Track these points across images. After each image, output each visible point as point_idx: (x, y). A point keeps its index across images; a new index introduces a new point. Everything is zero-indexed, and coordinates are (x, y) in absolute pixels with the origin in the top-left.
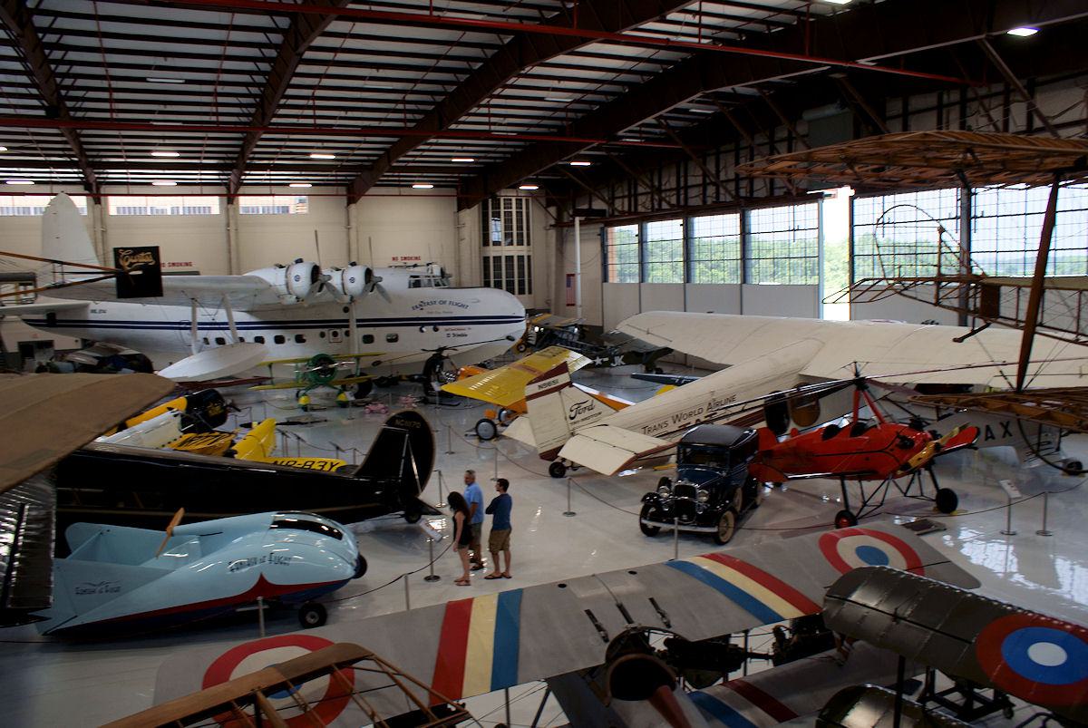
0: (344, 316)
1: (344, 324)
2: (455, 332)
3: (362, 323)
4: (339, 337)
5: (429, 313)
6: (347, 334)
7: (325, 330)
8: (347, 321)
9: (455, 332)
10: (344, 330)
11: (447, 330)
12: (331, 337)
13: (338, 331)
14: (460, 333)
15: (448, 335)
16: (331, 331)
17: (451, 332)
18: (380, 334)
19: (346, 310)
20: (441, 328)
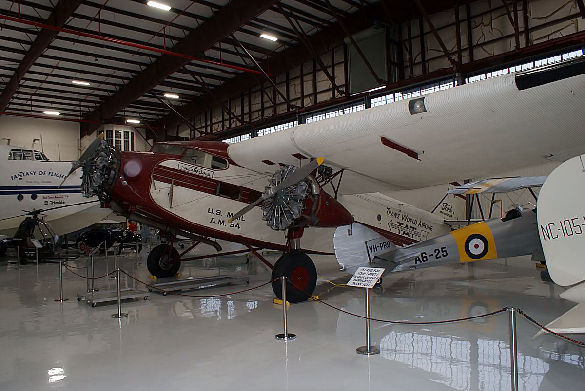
2: (53, 200)
9: (51, 199)
14: (57, 200)
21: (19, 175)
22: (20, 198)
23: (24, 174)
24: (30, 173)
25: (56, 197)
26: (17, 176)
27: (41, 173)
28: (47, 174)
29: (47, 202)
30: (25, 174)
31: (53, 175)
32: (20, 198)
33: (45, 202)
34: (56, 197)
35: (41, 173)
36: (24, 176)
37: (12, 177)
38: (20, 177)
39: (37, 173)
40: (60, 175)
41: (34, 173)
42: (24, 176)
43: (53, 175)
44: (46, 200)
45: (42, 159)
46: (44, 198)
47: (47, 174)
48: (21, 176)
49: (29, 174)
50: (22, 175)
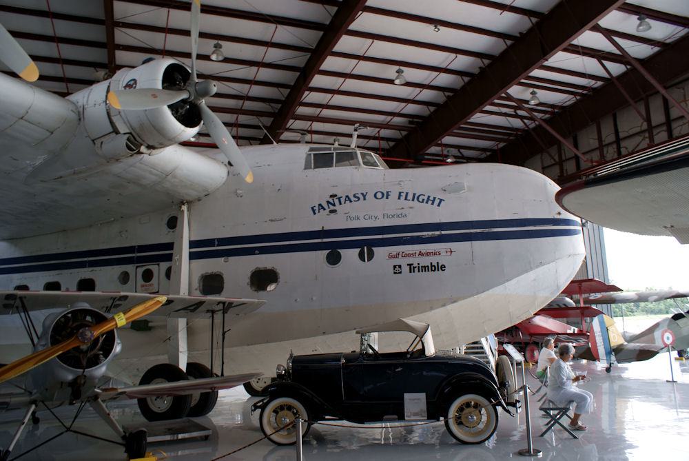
0: (157, 234)
1: (164, 252)
2: (415, 261)
3: (202, 250)
4: (154, 281)
5: (349, 218)
6: (168, 275)
7: (130, 268)
8: (170, 246)
9: (410, 260)
10: (164, 266)
11: (391, 256)
12: (140, 281)
13: (154, 268)
14: (425, 261)
15: (397, 269)
16: (141, 271)
17: (404, 262)
18: (237, 270)
19: (173, 223)
20: (380, 252)
21: (328, 202)
22: (334, 259)
23: (339, 199)
24: (354, 196)
25: (421, 254)
26: (325, 205)
27: (379, 195)
28: (394, 195)
29: (400, 266)
30: (343, 200)
31: (410, 197)
32: (334, 259)
33: (395, 267)
34: (421, 254)
35: (379, 195)
36: (340, 204)
37: (312, 208)
38: (332, 208)
39: (370, 196)
40: (426, 199)
41: (364, 196)
42: (340, 204)
43: (410, 197)
44: (397, 262)
45: (377, 166)
46: (391, 256)
47: (394, 195)
48: (334, 205)
49: (353, 199)
50: (337, 201)
